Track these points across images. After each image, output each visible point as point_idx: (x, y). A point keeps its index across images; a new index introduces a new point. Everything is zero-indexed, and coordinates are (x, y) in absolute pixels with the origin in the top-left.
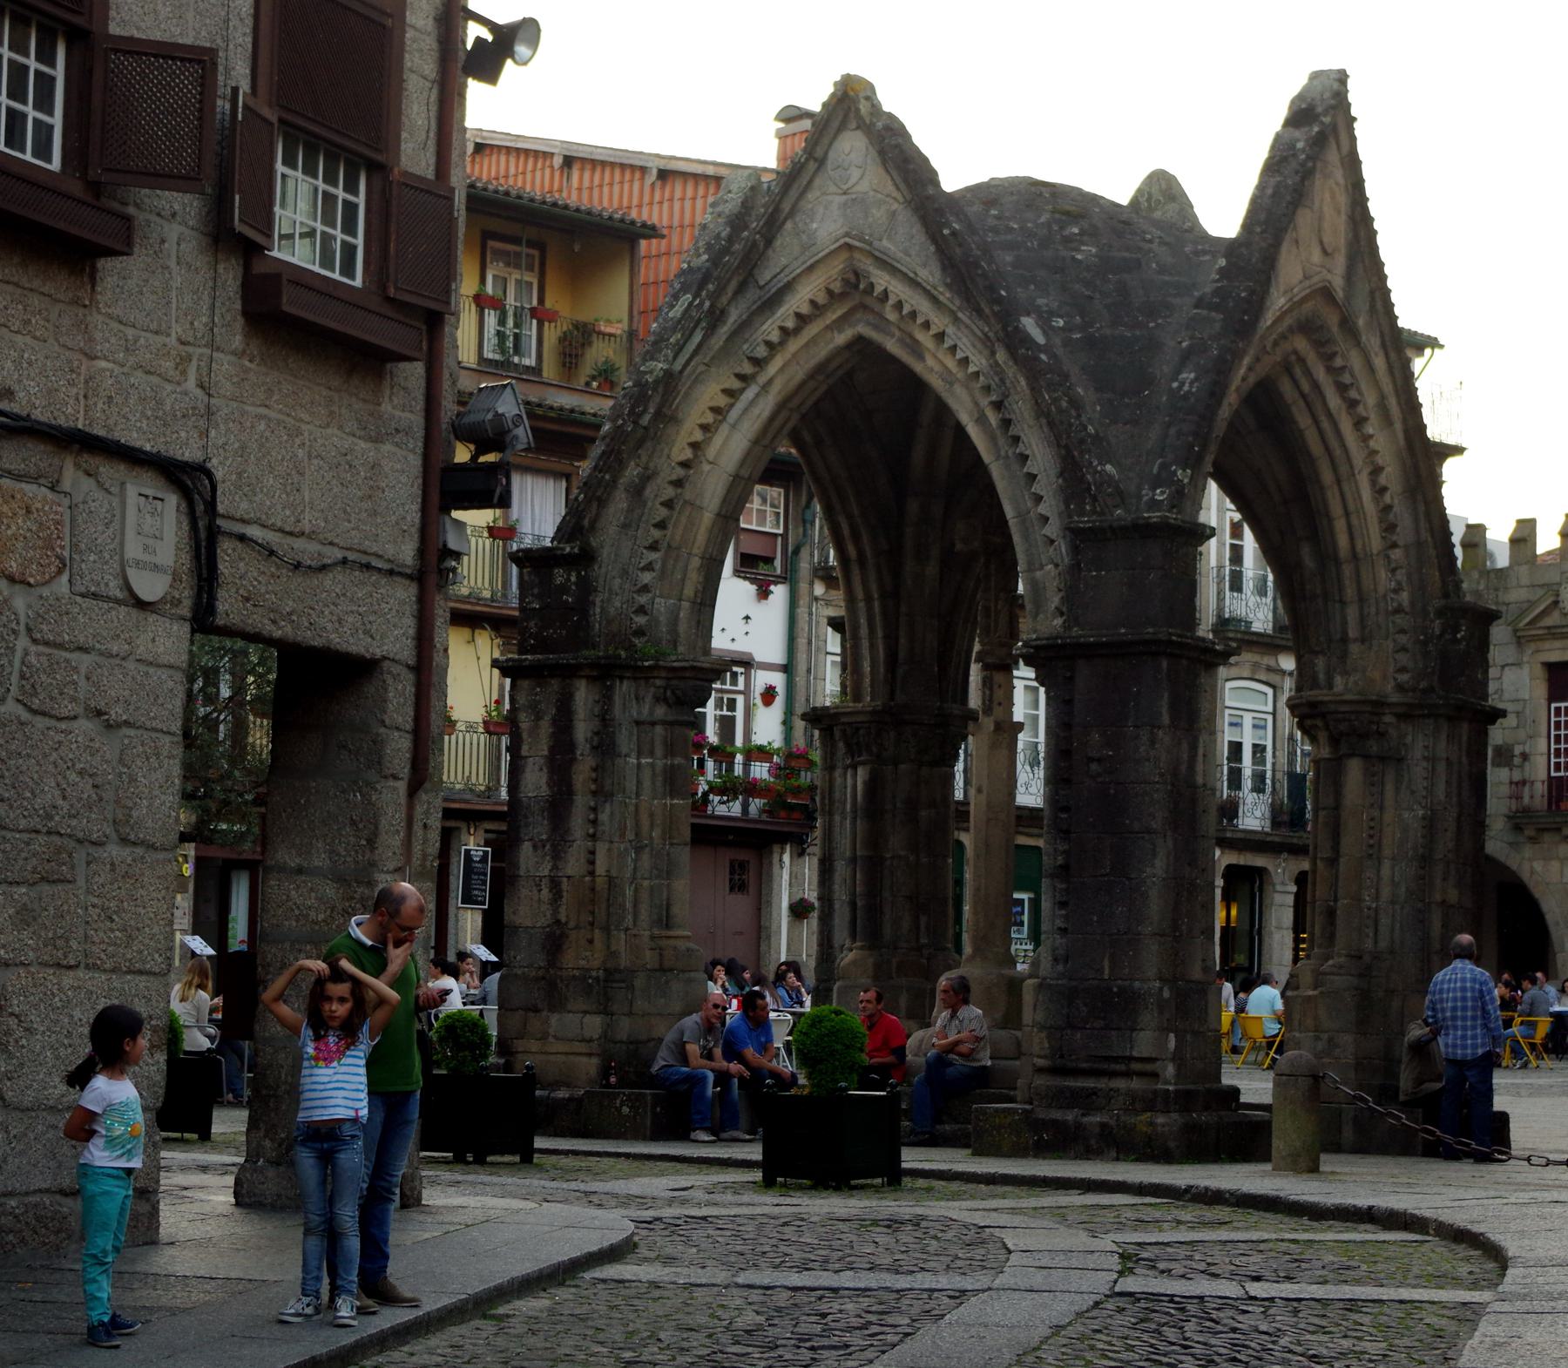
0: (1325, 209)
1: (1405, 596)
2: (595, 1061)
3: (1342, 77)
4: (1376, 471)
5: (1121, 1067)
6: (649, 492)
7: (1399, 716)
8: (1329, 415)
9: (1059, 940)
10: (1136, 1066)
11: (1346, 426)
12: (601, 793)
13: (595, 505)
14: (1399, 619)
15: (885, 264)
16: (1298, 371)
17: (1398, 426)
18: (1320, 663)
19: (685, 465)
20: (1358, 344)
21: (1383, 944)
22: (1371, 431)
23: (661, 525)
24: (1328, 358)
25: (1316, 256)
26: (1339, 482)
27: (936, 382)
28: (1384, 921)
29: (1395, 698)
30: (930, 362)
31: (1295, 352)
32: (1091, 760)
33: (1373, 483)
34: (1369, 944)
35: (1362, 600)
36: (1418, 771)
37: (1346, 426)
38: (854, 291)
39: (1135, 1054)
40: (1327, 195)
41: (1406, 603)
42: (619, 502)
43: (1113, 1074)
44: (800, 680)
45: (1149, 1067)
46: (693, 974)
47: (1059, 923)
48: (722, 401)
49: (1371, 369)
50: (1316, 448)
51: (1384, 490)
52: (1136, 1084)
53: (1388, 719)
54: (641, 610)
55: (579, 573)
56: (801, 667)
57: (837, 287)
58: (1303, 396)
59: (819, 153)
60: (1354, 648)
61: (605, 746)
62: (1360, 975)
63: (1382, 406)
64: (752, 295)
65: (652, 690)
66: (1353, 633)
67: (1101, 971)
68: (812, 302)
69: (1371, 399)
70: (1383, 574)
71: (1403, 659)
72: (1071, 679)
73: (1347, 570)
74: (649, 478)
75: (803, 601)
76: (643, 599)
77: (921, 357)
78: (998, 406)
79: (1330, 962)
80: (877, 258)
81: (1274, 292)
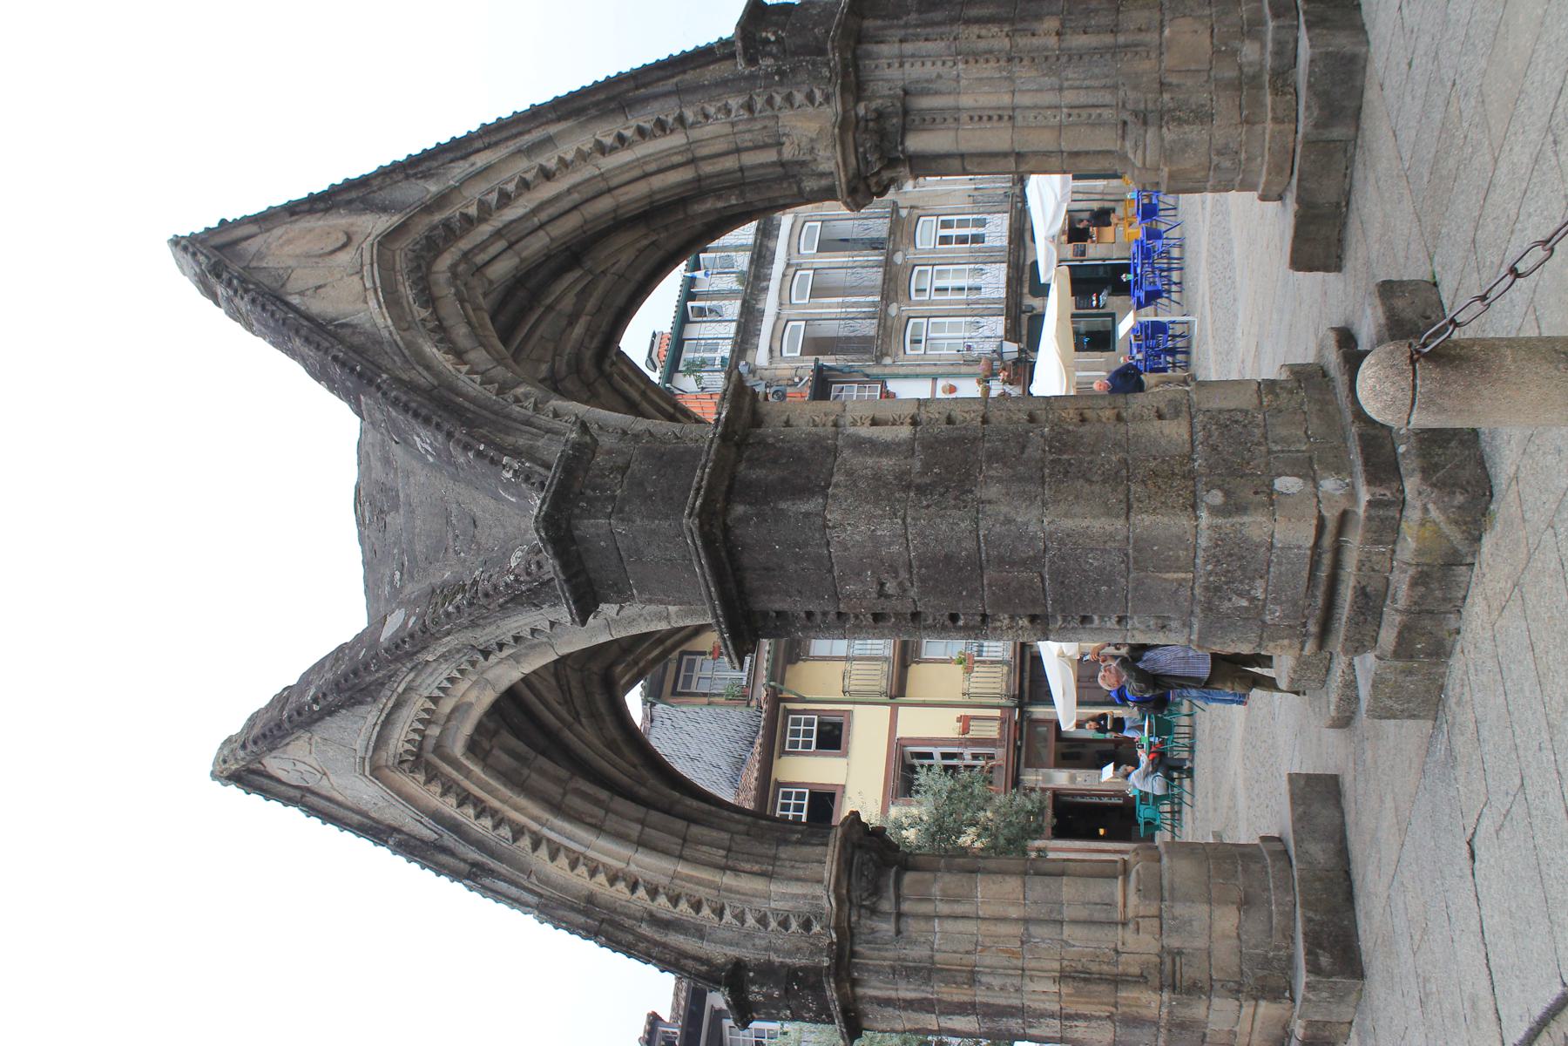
0: (298, 251)
1: (734, 102)
2: (1263, 1003)
3: (176, 242)
4: (602, 149)
5: (1327, 559)
6: (668, 916)
7: (858, 100)
9: (1134, 622)
10: (1327, 541)
11: (548, 191)
12: (972, 978)
13: (683, 961)
14: (759, 102)
15: (381, 741)
16: (481, 258)
17: (553, 129)
18: (810, 185)
19: (633, 887)
20: (454, 189)
21: (1108, 98)
23: (697, 906)
24: (469, 222)
25: (344, 257)
26: (610, 190)
27: (488, 697)
28: (1083, 98)
29: (837, 106)
30: (472, 697)
31: (453, 268)
32: (882, 594)
33: (613, 149)
34: (1107, 113)
35: (738, 151)
36: (914, 72)
37: (548, 191)
38: (420, 760)
39: (1311, 542)
40: (288, 249)
41: (741, 100)
42: (676, 940)
43: (1337, 565)
44: (941, 370)
45: (1331, 526)
46: (1165, 883)
47: (1112, 623)
48: (563, 861)
49: (488, 168)
50: (573, 221)
51: (621, 139)
52: (1355, 541)
54: (784, 924)
55: (753, 982)
56: (934, 370)
57: (421, 777)
58: (511, 246)
59: (298, 794)
60: (788, 153)
61: (926, 972)
62: (1145, 123)
63: (530, 151)
64: (449, 839)
65: (863, 921)
66: (770, 156)
67: (1180, 583)
68: (443, 794)
69: (522, 166)
70: (709, 130)
71: (799, 97)
72: (779, 614)
73: (708, 168)
74: (651, 915)
75: (895, 370)
76: (773, 924)
77: (470, 705)
78: (486, 654)
79: (1131, 156)
80: (375, 749)
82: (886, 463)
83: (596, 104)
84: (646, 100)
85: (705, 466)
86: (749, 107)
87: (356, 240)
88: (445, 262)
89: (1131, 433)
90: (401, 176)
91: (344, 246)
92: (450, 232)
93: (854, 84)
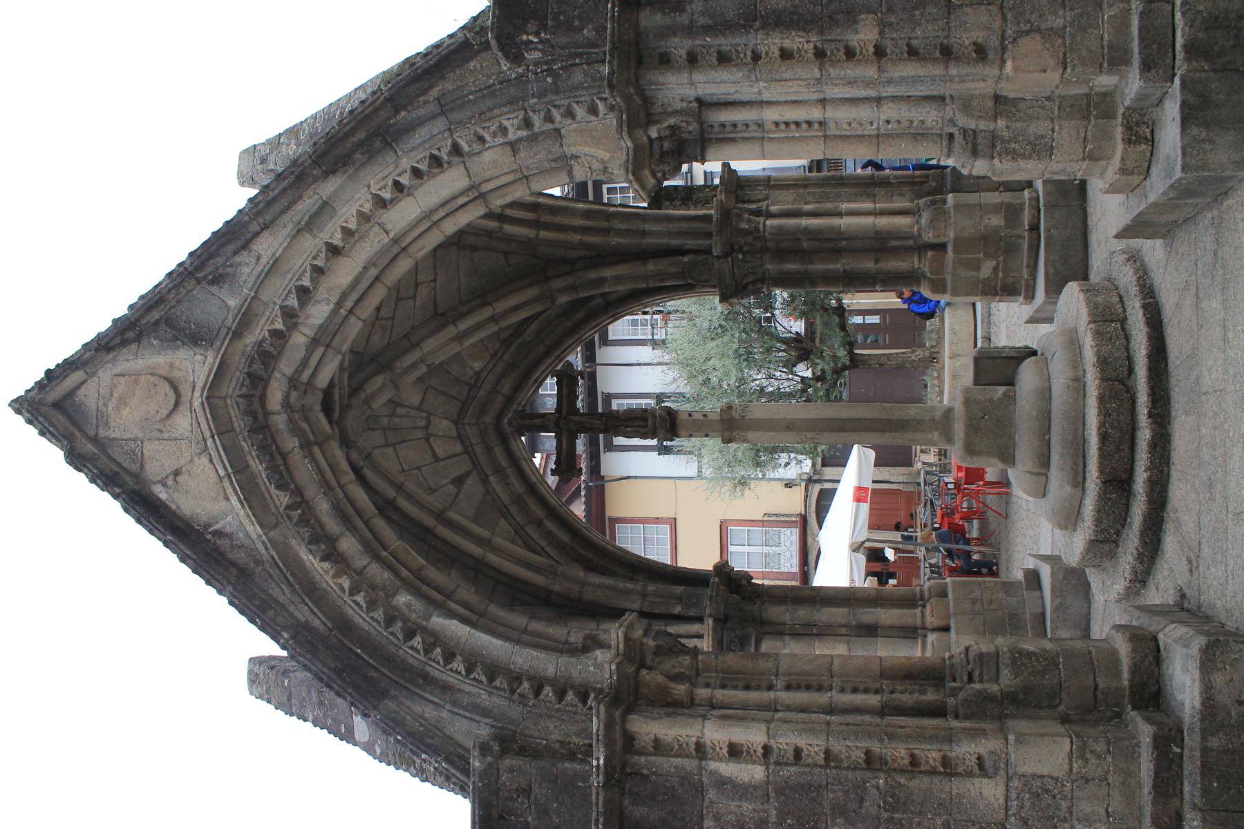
8: (339, 304)
14: (537, 121)
16: (305, 377)
22: (339, 235)
25: (182, 423)
53: (654, 135)
63: (310, 225)
71: (580, 112)
81: (227, 524)
82: (747, 807)
83: (359, 145)
84: (409, 129)
85: (597, 821)
86: (527, 123)
87: (185, 390)
88: (276, 395)
89: (955, 791)
90: (193, 282)
91: (177, 404)
92: (266, 357)
93: (639, 113)
